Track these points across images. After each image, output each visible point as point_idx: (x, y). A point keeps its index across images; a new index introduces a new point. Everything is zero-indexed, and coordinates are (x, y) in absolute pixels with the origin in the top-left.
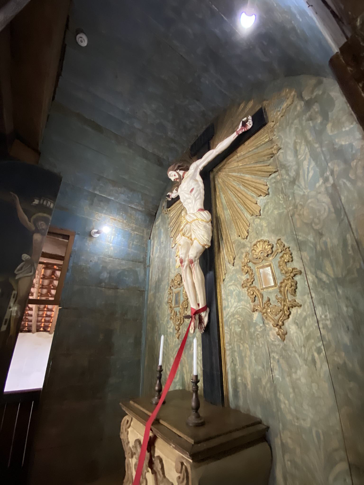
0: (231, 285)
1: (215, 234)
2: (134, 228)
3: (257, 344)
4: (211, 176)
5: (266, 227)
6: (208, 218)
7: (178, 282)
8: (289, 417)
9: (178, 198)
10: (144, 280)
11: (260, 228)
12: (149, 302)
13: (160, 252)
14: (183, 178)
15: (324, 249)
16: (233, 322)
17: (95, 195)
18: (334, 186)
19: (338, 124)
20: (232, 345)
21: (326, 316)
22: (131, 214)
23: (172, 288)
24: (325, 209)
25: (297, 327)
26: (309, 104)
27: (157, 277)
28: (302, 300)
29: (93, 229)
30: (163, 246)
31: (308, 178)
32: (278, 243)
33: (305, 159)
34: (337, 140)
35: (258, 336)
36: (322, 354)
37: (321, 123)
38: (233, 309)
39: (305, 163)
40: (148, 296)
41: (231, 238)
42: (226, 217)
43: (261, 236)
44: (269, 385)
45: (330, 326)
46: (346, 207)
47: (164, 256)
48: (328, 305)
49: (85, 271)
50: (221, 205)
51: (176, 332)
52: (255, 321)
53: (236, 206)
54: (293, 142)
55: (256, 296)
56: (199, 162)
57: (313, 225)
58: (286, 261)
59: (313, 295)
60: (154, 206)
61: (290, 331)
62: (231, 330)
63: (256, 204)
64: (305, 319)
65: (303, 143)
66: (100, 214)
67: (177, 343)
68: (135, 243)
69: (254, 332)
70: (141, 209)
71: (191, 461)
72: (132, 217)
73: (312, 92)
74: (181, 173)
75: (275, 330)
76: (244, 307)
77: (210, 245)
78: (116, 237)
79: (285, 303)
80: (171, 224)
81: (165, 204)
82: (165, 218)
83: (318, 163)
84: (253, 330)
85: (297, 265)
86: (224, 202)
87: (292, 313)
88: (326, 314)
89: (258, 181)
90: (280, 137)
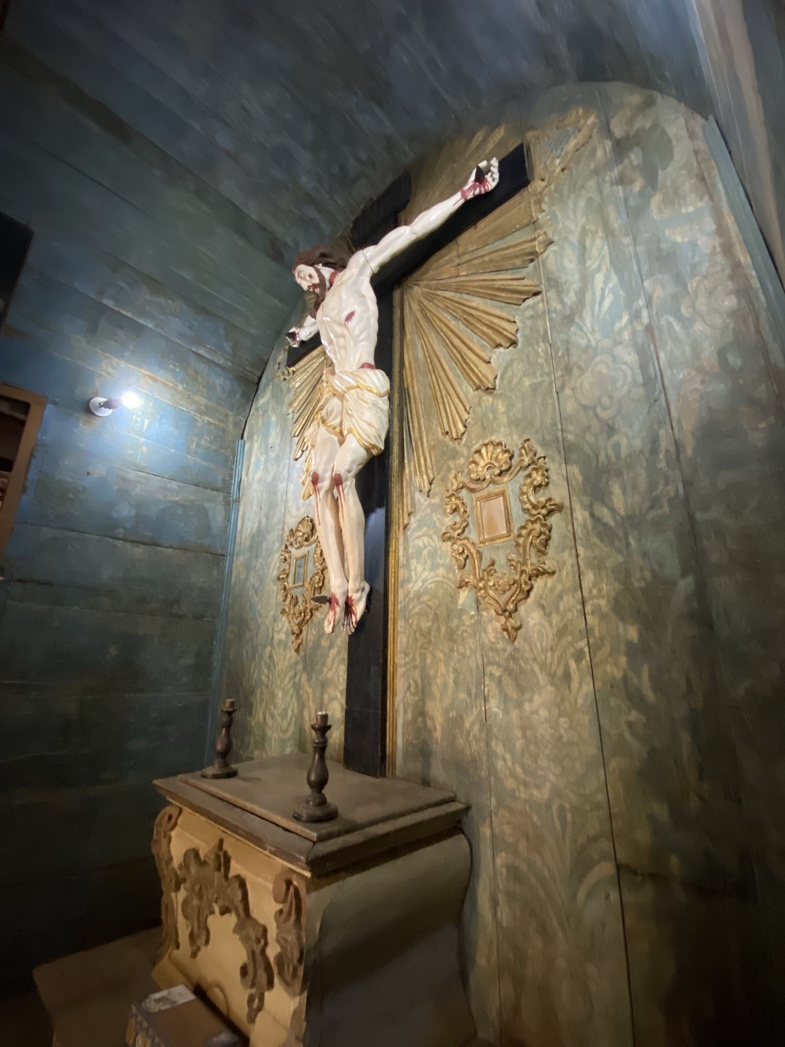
0: (420, 537)
1: (396, 429)
2: (203, 408)
3: (461, 649)
4: (397, 295)
5: (504, 413)
6: (382, 387)
7: (304, 534)
8: (510, 783)
9: (315, 341)
10: (225, 531)
11: (491, 416)
12: (233, 580)
13: (266, 469)
14: (331, 285)
15: (614, 459)
16: (416, 610)
17: (103, 309)
18: (649, 329)
19: (674, 197)
20: (411, 656)
21: (600, 590)
22: (196, 372)
23: (290, 548)
24: (625, 376)
25: (542, 613)
26: (621, 148)
27: (256, 526)
29: (97, 395)
30: (272, 455)
31: (600, 310)
33: (599, 268)
34: (667, 233)
36: (584, 662)
37: (641, 193)
38: (420, 584)
39: (599, 278)
40: (231, 568)
43: (492, 434)
44: (476, 728)
46: (667, 375)
47: (275, 479)
49: (71, 496)
51: (293, 637)
52: (462, 605)
54: (580, 229)
55: (467, 556)
56: (370, 251)
57: (599, 410)
58: (535, 483)
59: (581, 551)
60: (256, 352)
61: (528, 622)
62: (411, 626)
63: (489, 362)
64: (560, 597)
65: (600, 234)
66: (115, 360)
67: (293, 660)
68: (203, 443)
70: (222, 362)
71: (308, 874)
72: (200, 379)
73: (632, 120)
74: (327, 272)
75: (499, 621)
77: (382, 448)
78: (157, 425)
79: (524, 568)
80: (295, 405)
81: (282, 357)
82: (281, 390)
83: (626, 278)
85: (558, 493)
87: (536, 586)
89: (497, 312)
90: (554, 216)
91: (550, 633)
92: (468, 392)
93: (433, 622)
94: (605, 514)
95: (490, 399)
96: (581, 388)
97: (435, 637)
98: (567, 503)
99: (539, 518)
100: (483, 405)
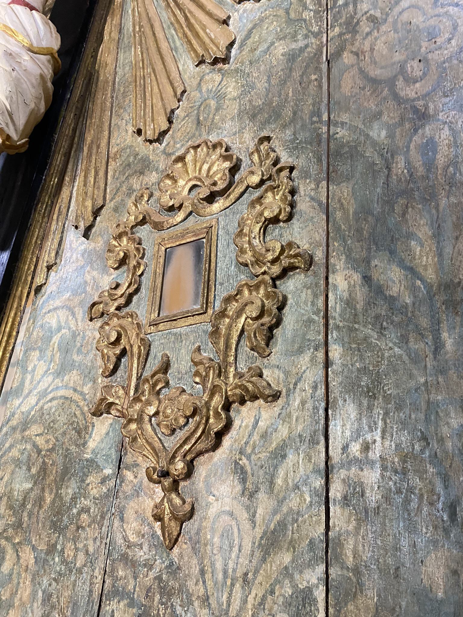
0: (56, 309)
3: (69, 553)
15: (421, 171)
16: (15, 453)
21: (366, 448)
25: (239, 488)
28: (287, 373)
32: (258, 151)
35: (84, 516)
38: (32, 400)
41: (113, 141)
42: (120, 71)
45: (373, 497)
48: (387, 399)
50: (115, 35)
52: (93, 451)
53: (160, 35)
55: (124, 352)
57: (400, 83)
63: (225, 22)
64: (280, 454)
69: (74, 499)
76: (69, 393)
84: (70, 491)
85: (303, 234)
86: (129, 25)
87: (237, 423)
88: (369, 437)
91: (248, 538)
92: (185, 71)
93: (35, 483)
94: (393, 278)
95: (217, 78)
96: (372, 50)
97: (30, 516)
98: (319, 255)
99: (263, 282)
100: (204, 89)
